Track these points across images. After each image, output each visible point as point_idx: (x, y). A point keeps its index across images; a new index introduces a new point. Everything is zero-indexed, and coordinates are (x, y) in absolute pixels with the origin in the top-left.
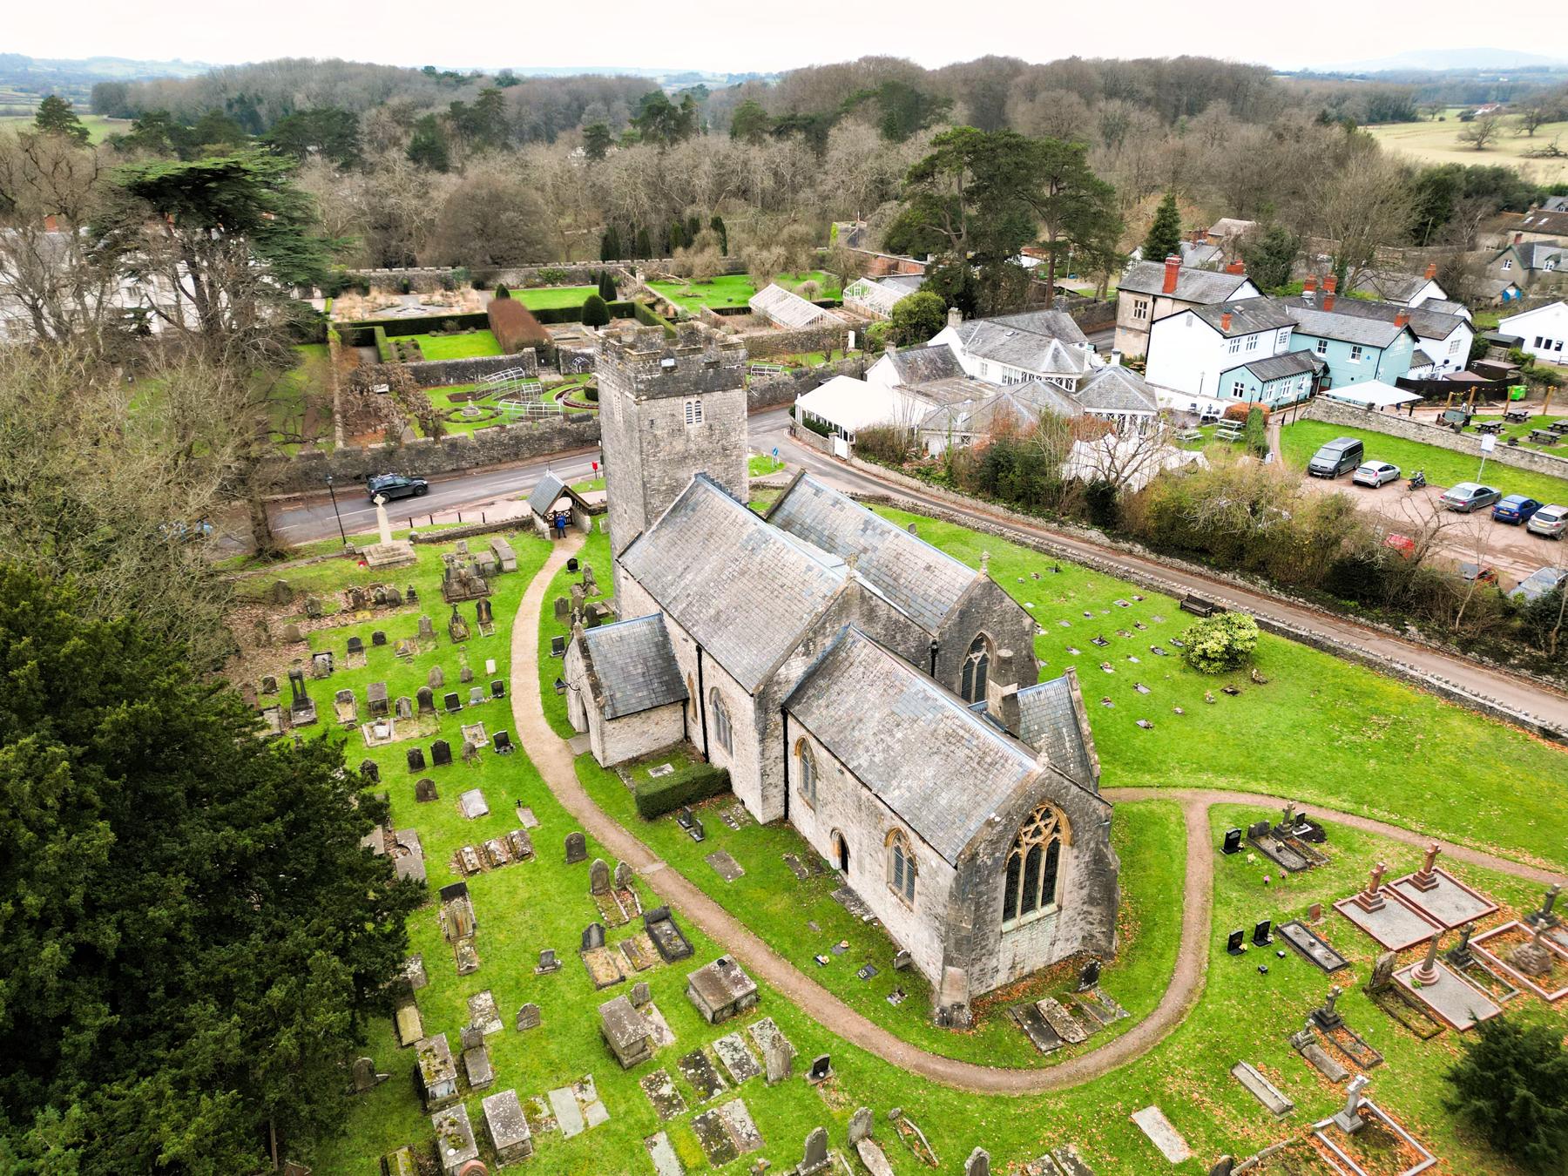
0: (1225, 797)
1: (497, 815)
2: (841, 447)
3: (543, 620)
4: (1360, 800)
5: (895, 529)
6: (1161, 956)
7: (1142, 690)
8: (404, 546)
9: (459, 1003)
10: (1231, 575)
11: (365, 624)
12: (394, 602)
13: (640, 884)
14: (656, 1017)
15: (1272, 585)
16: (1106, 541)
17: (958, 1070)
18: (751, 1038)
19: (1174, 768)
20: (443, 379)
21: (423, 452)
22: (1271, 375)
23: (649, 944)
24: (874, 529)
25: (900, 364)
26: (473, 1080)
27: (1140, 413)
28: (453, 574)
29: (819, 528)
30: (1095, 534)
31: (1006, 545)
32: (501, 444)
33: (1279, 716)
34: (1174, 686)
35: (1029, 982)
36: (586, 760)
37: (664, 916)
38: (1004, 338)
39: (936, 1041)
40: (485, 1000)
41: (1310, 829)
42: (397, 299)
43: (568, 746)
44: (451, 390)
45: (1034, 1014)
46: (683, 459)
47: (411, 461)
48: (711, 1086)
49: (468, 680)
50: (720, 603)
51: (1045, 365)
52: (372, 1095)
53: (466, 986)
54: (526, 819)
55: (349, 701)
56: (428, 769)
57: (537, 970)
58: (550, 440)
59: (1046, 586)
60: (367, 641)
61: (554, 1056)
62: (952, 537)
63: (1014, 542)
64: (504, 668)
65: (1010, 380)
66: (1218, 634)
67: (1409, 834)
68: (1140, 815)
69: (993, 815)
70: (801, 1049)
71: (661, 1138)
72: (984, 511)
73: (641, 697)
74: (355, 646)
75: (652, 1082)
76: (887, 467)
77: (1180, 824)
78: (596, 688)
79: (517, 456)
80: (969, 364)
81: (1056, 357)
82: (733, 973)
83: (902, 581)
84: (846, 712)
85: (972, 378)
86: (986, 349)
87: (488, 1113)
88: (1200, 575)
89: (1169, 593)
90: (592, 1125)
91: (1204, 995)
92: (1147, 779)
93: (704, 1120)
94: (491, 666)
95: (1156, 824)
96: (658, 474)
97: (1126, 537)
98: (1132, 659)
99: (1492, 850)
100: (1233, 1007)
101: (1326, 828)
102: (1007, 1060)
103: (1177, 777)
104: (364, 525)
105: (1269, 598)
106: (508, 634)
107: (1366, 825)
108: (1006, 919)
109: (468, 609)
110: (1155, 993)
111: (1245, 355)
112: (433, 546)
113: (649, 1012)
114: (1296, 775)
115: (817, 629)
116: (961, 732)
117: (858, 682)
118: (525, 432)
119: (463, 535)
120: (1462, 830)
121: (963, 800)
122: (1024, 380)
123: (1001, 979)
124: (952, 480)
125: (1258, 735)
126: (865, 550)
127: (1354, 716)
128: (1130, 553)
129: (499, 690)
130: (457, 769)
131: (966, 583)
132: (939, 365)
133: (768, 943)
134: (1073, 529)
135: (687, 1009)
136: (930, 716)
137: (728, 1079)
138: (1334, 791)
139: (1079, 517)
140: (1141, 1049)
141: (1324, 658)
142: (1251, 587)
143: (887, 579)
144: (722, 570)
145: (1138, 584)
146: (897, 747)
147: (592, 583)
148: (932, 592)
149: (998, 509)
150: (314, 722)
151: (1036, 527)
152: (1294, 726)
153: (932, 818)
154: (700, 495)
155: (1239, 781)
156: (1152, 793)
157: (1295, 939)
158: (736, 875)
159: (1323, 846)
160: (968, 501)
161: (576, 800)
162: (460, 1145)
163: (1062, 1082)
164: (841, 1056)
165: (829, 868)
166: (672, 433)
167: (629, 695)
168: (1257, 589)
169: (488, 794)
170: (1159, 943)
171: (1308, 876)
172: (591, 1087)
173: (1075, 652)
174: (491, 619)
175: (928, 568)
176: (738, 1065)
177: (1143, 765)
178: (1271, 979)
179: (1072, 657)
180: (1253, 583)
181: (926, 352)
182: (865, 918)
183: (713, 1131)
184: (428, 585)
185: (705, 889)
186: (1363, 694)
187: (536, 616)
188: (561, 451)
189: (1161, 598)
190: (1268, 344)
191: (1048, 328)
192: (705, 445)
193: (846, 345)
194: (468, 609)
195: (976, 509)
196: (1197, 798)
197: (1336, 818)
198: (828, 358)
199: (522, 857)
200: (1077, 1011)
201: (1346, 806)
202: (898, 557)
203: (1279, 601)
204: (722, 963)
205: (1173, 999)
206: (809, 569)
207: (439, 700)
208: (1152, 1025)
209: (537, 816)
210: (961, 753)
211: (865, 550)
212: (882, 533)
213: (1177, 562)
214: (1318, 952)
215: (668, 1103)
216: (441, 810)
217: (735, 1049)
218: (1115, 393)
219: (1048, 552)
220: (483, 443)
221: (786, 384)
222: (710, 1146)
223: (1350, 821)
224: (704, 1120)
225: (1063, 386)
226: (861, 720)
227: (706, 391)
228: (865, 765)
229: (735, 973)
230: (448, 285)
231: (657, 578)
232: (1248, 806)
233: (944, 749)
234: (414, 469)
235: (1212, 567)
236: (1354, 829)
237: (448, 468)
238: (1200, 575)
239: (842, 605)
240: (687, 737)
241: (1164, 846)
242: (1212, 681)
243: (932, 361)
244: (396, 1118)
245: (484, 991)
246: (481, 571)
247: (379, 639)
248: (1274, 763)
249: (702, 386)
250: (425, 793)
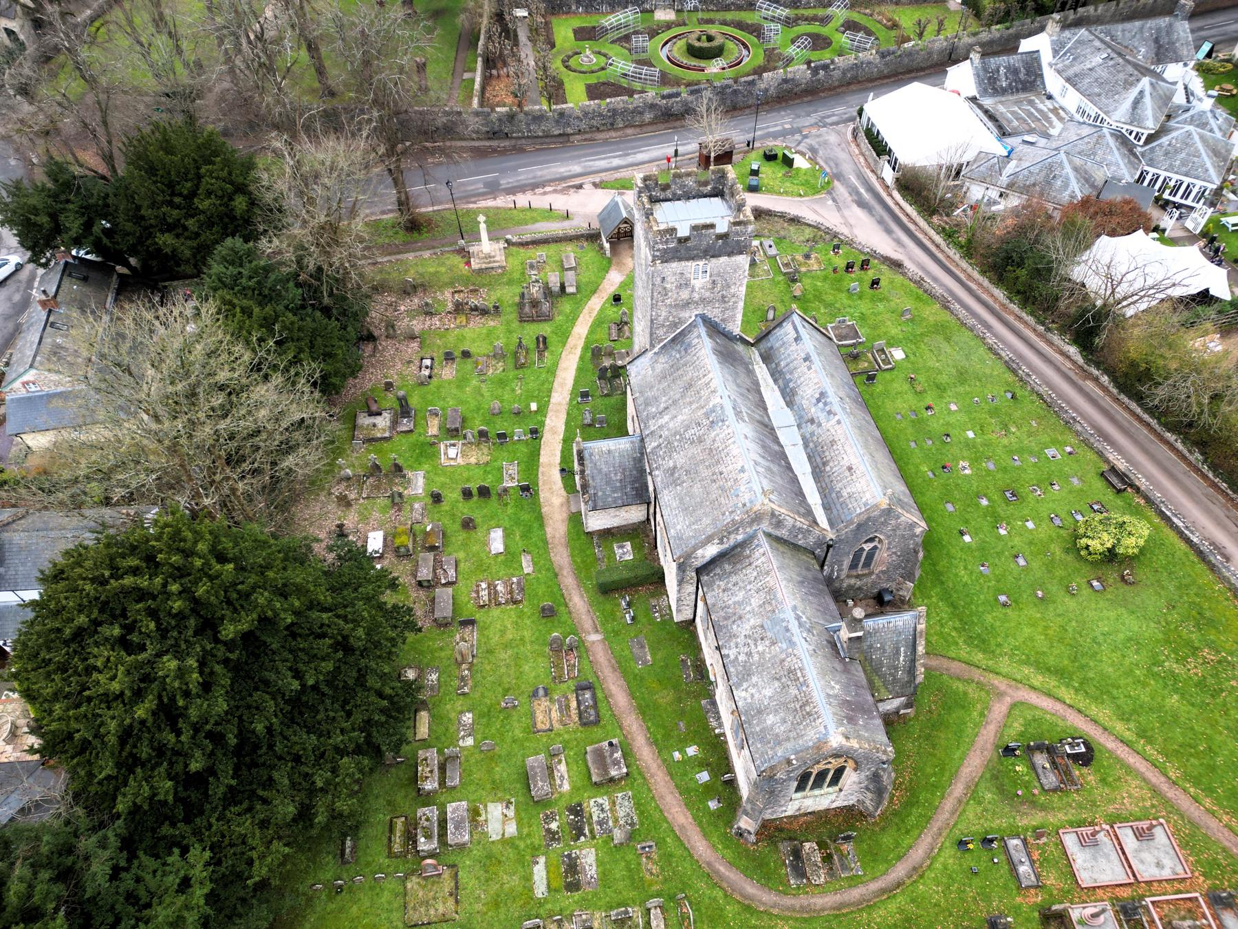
0: (1033, 698)
1: (510, 556)
2: (889, 175)
3: (582, 358)
4: (1142, 733)
5: (841, 415)
6: (907, 832)
7: (1021, 562)
9: (453, 715)
10: (1174, 437)
13: (582, 649)
14: (563, 767)
15: (1205, 461)
16: (1081, 361)
17: (733, 875)
18: (614, 803)
19: (1006, 654)
20: (574, 8)
21: (539, 118)
23: (574, 704)
24: (825, 404)
25: (981, 73)
26: (449, 783)
27: (1199, 183)
28: (526, 296)
29: (788, 376)
30: (1073, 350)
31: (982, 350)
32: (600, 115)
33: (1123, 624)
34: (1050, 566)
35: (808, 818)
37: (590, 687)
38: (1098, 59)
39: (727, 847)
40: (468, 718)
41: (1083, 750)
43: (568, 502)
44: (577, 22)
45: (797, 853)
46: (686, 305)
47: (528, 125)
48: (580, 833)
50: (680, 459)
51: (1119, 116)
52: (393, 770)
53: (459, 704)
55: (437, 415)
56: (475, 498)
57: (503, 704)
58: (641, 113)
59: (994, 412)
60: (457, 353)
61: (497, 777)
62: (940, 329)
63: (990, 349)
65: (1084, 112)
66: (1105, 536)
67: (1163, 779)
68: (956, 693)
69: (793, 757)
70: (642, 824)
71: (542, 860)
72: (986, 291)
75: (547, 817)
76: (919, 213)
77: (982, 715)
79: (612, 127)
80: (1053, 81)
81: (1137, 103)
82: (616, 755)
83: (828, 468)
84: (735, 603)
85: (1050, 97)
86: (1071, 72)
87: (449, 815)
88: (1148, 425)
89: (1100, 454)
90: (507, 835)
91: (921, 876)
92: (979, 657)
93: (569, 856)
95: (963, 707)
96: (664, 314)
97: (1098, 365)
98: (1030, 525)
99: (1225, 818)
100: (937, 892)
101: (1097, 754)
102: (767, 877)
103: (1004, 665)
104: (483, 194)
105: (1197, 470)
107: (1133, 760)
108: (796, 791)
110: (887, 861)
112: (522, 250)
113: (560, 762)
114: (1102, 691)
115: (735, 527)
116: (799, 674)
117: (750, 583)
118: (621, 105)
120: (1210, 791)
121: (780, 729)
122: (1096, 119)
123: (789, 813)
124: (969, 250)
125: (1094, 640)
126: (812, 421)
127: (1189, 644)
128: (1096, 380)
129: (535, 433)
131: (871, 502)
132: (1022, 76)
133: (648, 729)
134: (1056, 339)
135: (583, 767)
136: (784, 646)
137: (591, 831)
138: (1124, 717)
139: (1063, 331)
140: (859, 903)
141: (1200, 567)
142: (1188, 455)
143: (818, 460)
144: (687, 428)
145: (1078, 434)
146: (756, 657)
147: (626, 323)
148: (845, 494)
149: (999, 294)
150: (411, 431)
151: (1026, 323)
152: (1130, 639)
153: (758, 729)
154: (692, 338)
155: (1052, 682)
156: (976, 674)
157: (1012, 852)
158: (645, 662)
159: (1085, 770)
160: (976, 274)
161: (561, 557)
162: (428, 837)
163: (794, 910)
164: (664, 839)
165: (708, 677)
166: (680, 287)
168: (1191, 458)
169: (507, 536)
170: (912, 819)
171: (1055, 798)
172: (512, 808)
173: (984, 502)
174: (546, 348)
175: (850, 469)
176: (600, 823)
177: (982, 643)
178: (976, 881)
179: (978, 505)
180: (1190, 451)
181: (1013, 60)
182: (717, 731)
183: (572, 866)
185: (621, 668)
186: (1211, 623)
187: (579, 352)
188: (650, 124)
189: (1091, 456)
191: (1157, 41)
192: (708, 294)
195: (980, 285)
196: (1009, 691)
197: (1110, 744)
198: (921, 35)
199: (515, 602)
200: (828, 859)
201: (1128, 735)
202: (833, 442)
203: (1204, 477)
204: (611, 744)
205: (900, 871)
206: (742, 470)
208: (874, 886)
209: (535, 564)
210: (793, 691)
211: (812, 421)
212: (830, 412)
213: (1133, 406)
214: (1024, 869)
215: (552, 836)
217: (602, 810)
218: (1183, 155)
219: (1014, 372)
220: (586, 114)
221: (869, 63)
222: (566, 877)
223: (1122, 752)
224: (569, 856)
225: (1132, 138)
226: (740, 618)
227: (713, 256)
228: (732, 657)
229: (618, 755)
231: (647, 404)
232: (1046, 712)
233: (784, 680)
234: (530, 131)
235: (1160, 423)
236: (1119, 760)
237: (557, 132)
238: (1148, 425)
240: (648, 519)
241: (959, 733)
242: (1086, 569)
243: (1015, 71)
244: (403, 793)
245: (469, 711)
246: (548, 292)
248: (1091, 675)
249: (710, 253)
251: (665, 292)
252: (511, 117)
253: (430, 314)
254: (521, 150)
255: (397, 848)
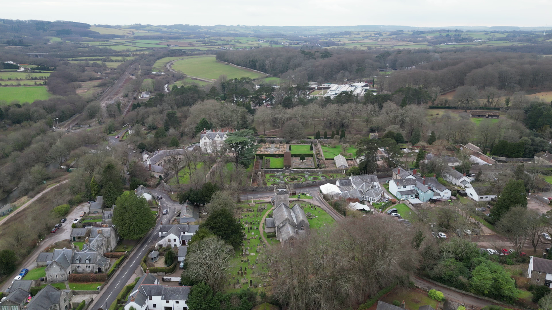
8: (254, 204)
11: (247, 213)
12: (251, 211)
21: (262, 188)
22: (404, 194)
36: (264, 232)
42: (270, 145)
46: (281, 201)
49: (256, 222)
54: (257, 236)
60: (247, 215)
64: (260, 221)
73: (270, 226)
74: (246, 216)
78: (266, 224)
94: (259, 220)
106: (262, 217)
109: (259, 213)
111: (402, 189)
115: (284, 222)
119: (262, 203)
129: (259, 223)
130: (252, 230)
132: (348, 183)
134: (342, 216)
149: (335, 211)
167: (269, 226)
169: (254, 233)
184: (256, 209)
190: (409, 188)
191: (371, 178)
193: (344, 172)
194: (259, 213)
207: (252, 223)
216: (250, 234)
220: (270, 187)
230: (281, 143)
239: (286, 220)
243: (347, 182)
247: (248, 215)
250: (249, 232)
251: (278, 199)
252: (257, 187)
253: (242, 211)
254: (258, 193)
255: (240, 255)
